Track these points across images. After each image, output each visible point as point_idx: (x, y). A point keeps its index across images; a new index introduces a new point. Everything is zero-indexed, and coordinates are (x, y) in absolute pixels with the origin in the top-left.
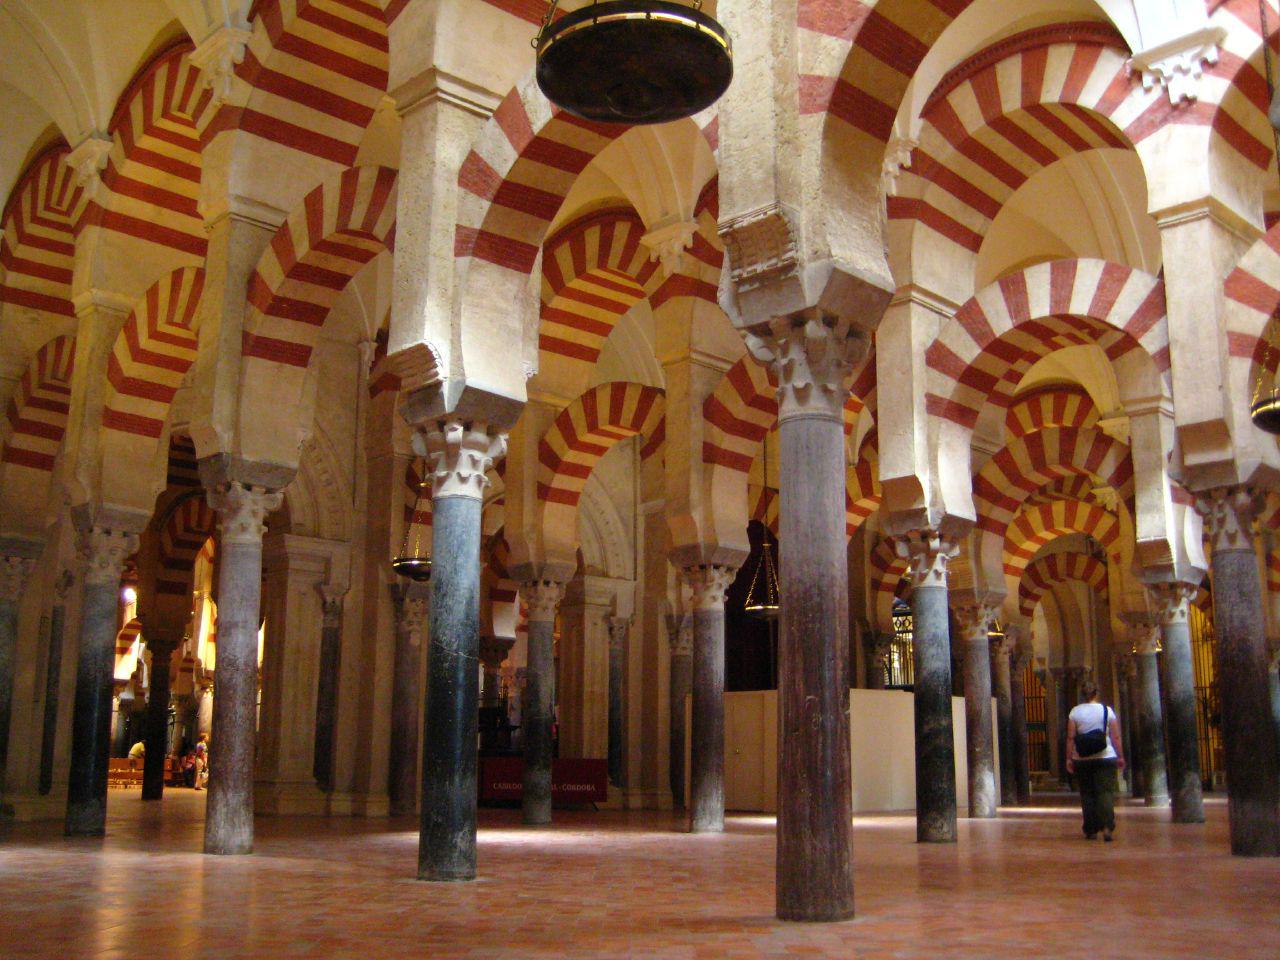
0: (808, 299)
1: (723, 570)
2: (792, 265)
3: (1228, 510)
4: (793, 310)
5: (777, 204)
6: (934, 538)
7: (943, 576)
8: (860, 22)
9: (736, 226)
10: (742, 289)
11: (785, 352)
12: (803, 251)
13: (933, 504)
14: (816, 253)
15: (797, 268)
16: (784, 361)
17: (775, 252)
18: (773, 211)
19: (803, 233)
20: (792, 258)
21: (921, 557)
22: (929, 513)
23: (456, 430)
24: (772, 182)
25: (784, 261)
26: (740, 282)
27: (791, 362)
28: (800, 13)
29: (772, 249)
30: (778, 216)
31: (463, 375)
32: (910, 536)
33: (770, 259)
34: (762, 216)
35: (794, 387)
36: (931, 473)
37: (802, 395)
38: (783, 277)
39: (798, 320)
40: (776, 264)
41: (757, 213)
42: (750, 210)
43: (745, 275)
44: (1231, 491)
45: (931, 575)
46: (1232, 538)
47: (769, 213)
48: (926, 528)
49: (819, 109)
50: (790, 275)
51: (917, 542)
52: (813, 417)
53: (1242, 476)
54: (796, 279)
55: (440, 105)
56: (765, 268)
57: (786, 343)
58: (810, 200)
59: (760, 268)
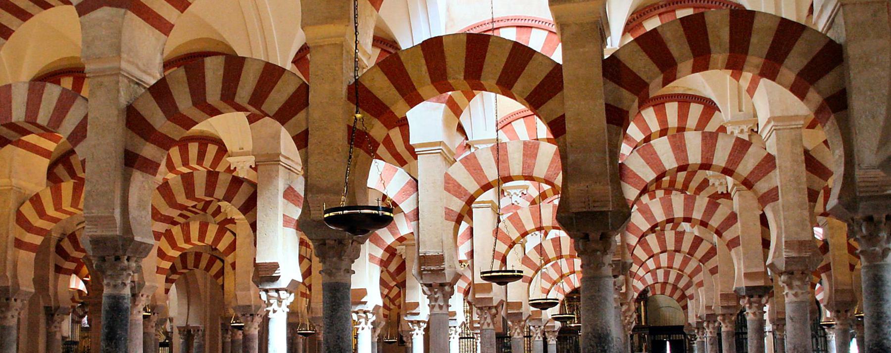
2: (444, 269)
3: (488, 314)
8: (467, 197)
10: (424, 272)
11: (436, 293)
12: (446, 265)
16: (436, 296)
26: (425, 270)
30: (442, 255)
39: (442, 285)
41: (436, 252)
44: (490, 308)
46: (489, 325)
49: (453, 221)
52: (444, 314)
53: (495, 304)
54: (444, 273)
55: (280, 167)
59: (432, 268)
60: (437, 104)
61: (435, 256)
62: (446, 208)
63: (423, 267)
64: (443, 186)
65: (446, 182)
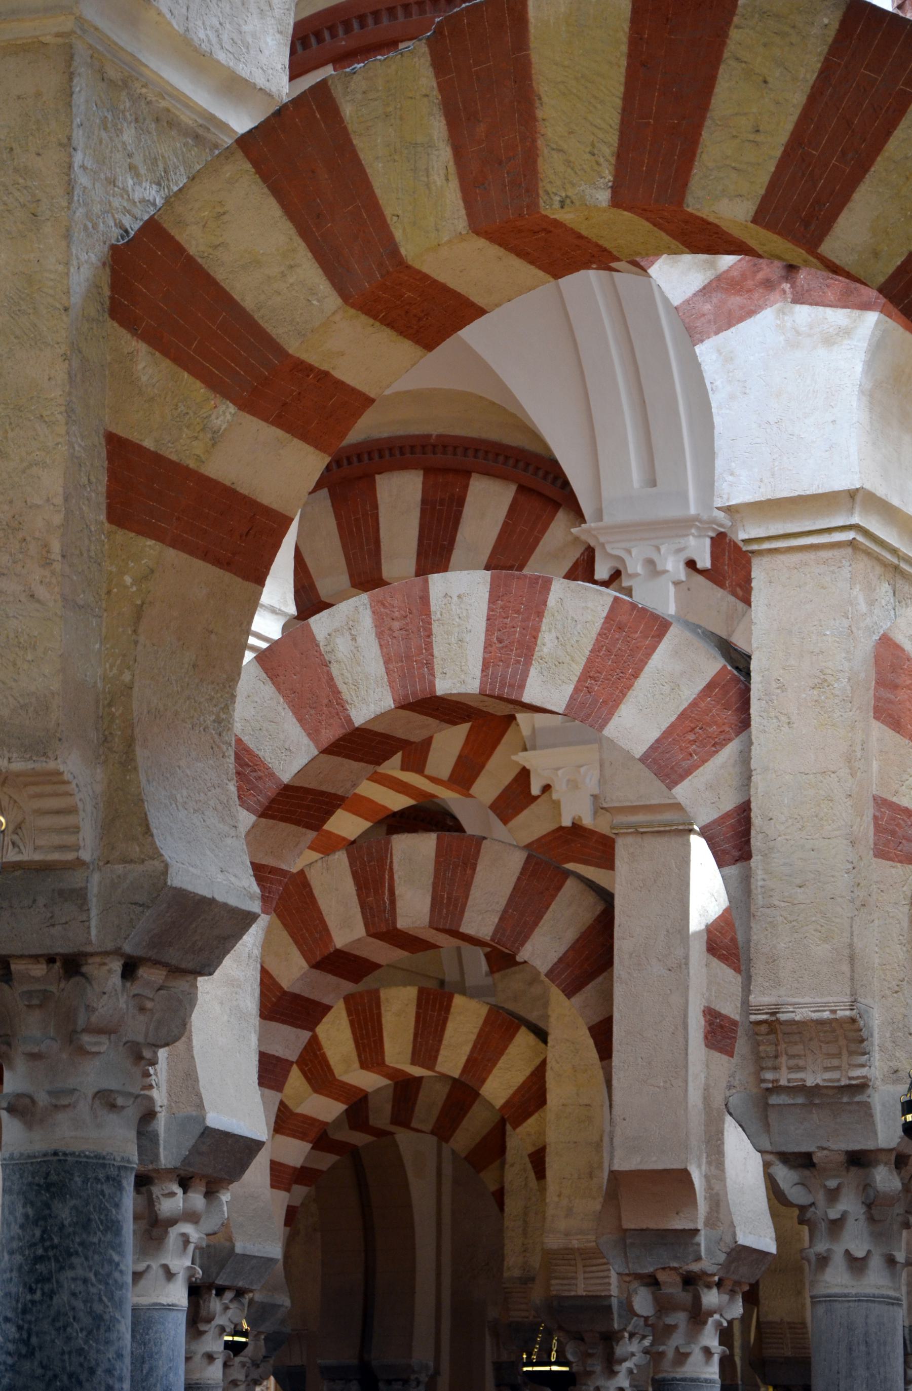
0: (880, 1135)
1: (229, 1295)
2: (862, 1087)
4: (857, 1147)
5: (854, 1003)
6: (709, 1286)
7: (716, 1358)
9: (783, 1017)
10: (774, 1100)
11: (833, 1195)
13: (711, 1221)
14: (896, 1071)
15: (870, 1091)
16: (834, 1214)
17: (835, 1062)
18: (848, 1013)
19: (876, 1039)
20: (864, 1077)
21: (680, 1318)
22: (702, 1239)
23: (172, 1194)
24: (846, 968)
25: (850, 1078)
26: (777, 1089)
27: (844, 1215)
28: (877, 699)
29: (830, 1056)
31: (201, 1106)
32: (662, 1277)
33: (826, 1069)
34: (826, 1015)
35: (847, 1252)
36: (709, 1163)
37: (856, 1265)
38: (845, 1100)
40: (839, 1080)
42: (807, 999)
43: (783, 1082)
45: (697, 1356)
47: (840, 1014)
48: (695, 1267)
50: (857, 1099)
51: (672, 1287)
52: (872, 1299)
54: (866, 1109)
56: (819, 1081)
57: (838, 1189)
58: (888, 992)
59: (811, 1080)
60: (837, 317)
61: (821, 1023)
62: (881, 803)
63: (769, 1076)
64: (867, 697)
65: (881, 682)
